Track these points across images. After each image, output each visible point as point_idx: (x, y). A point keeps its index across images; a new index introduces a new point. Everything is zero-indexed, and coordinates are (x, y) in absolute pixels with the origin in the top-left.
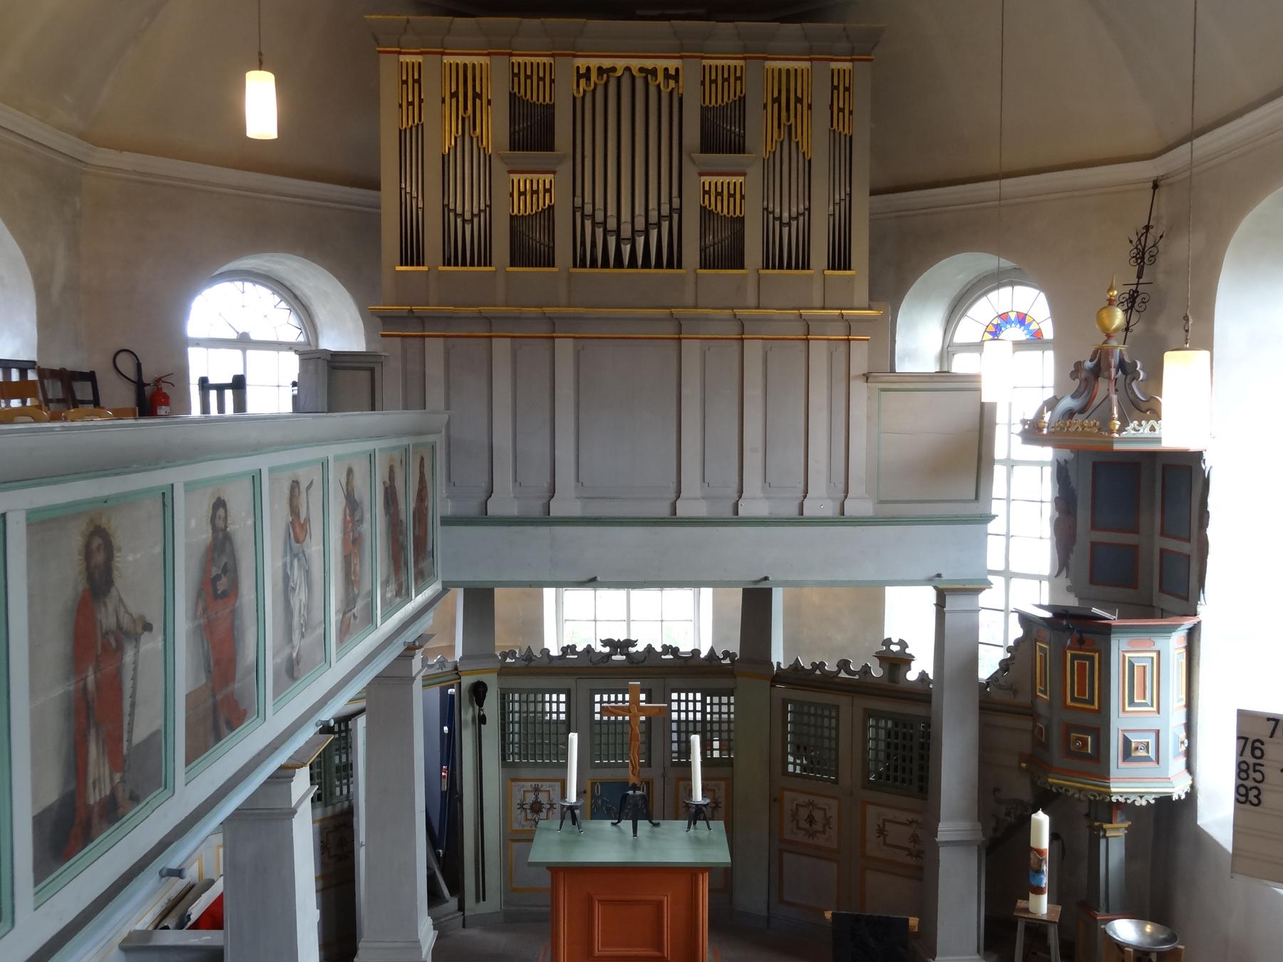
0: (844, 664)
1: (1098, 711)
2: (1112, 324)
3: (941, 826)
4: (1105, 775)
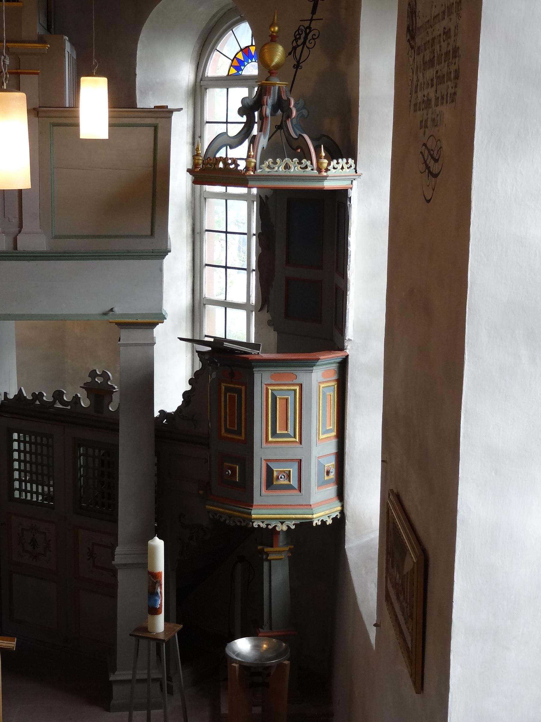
0: (58, 395)
2: (272, 61)
3: (118, 550)
4: (249, 502)
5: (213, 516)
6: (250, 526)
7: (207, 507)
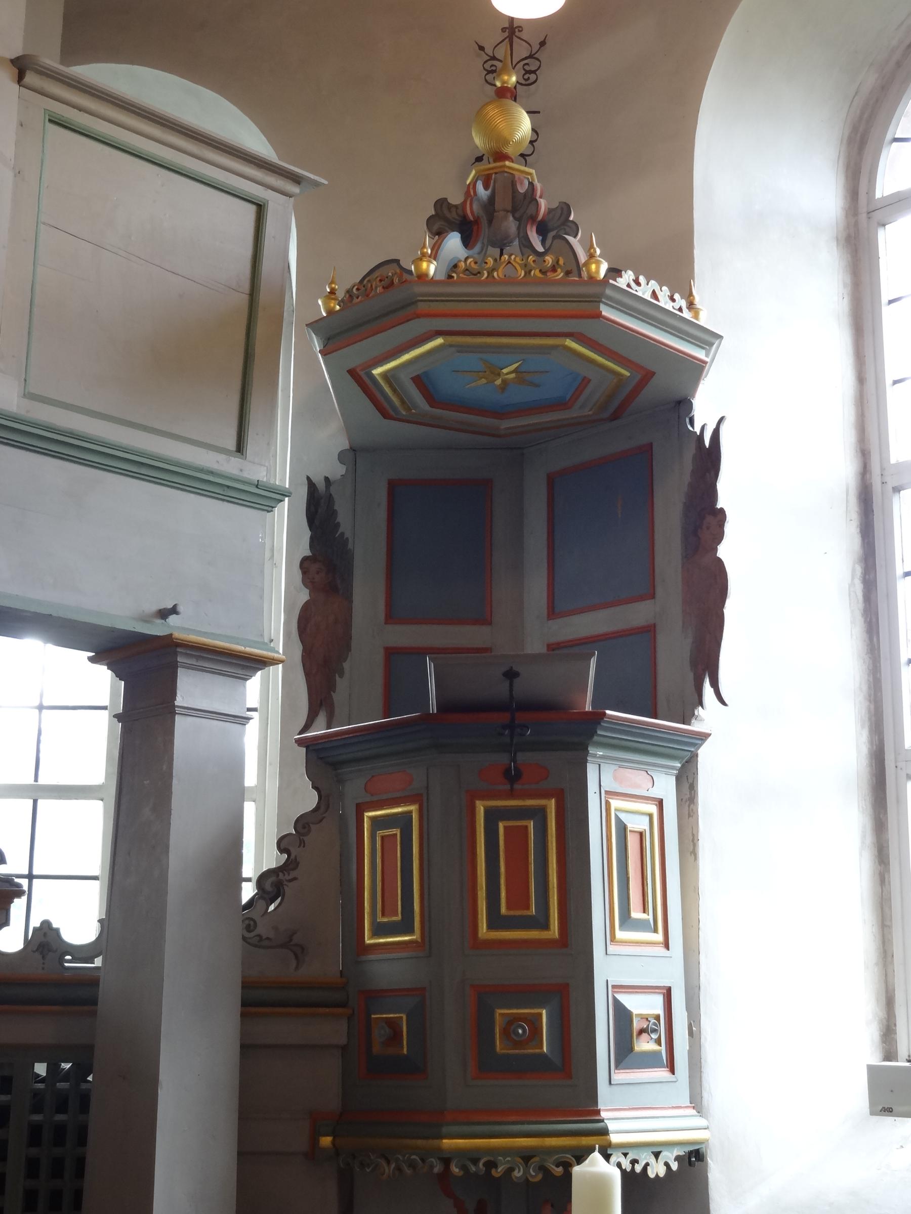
5: (464, 1168)
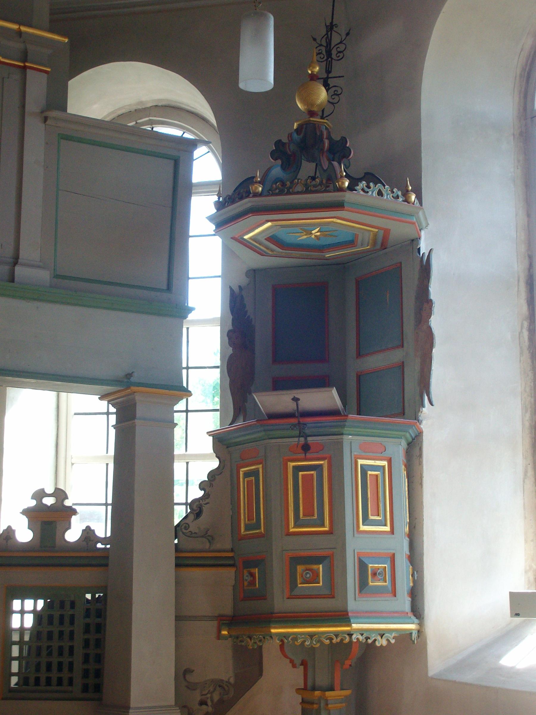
1: (330, 532)
6: (347, 640)
7: (273, 631)
